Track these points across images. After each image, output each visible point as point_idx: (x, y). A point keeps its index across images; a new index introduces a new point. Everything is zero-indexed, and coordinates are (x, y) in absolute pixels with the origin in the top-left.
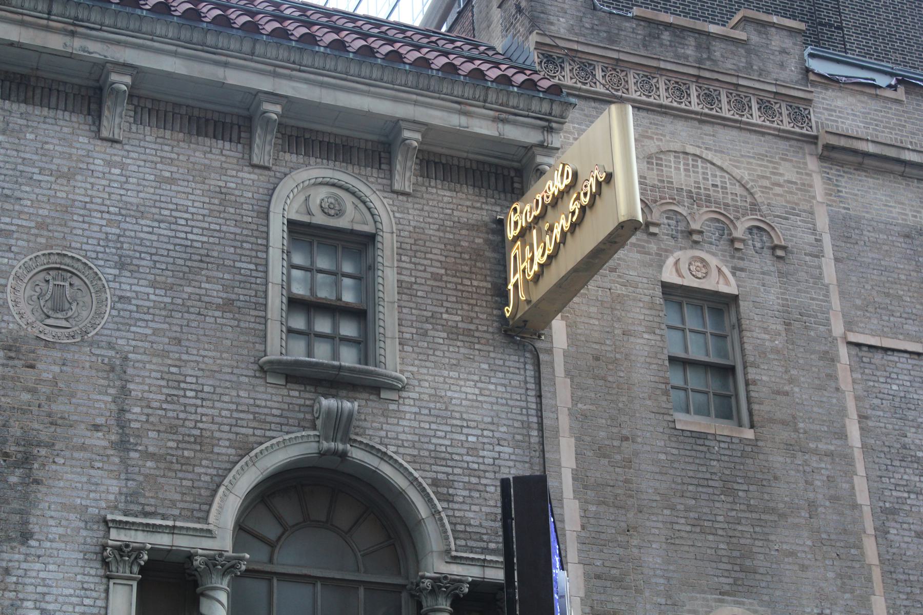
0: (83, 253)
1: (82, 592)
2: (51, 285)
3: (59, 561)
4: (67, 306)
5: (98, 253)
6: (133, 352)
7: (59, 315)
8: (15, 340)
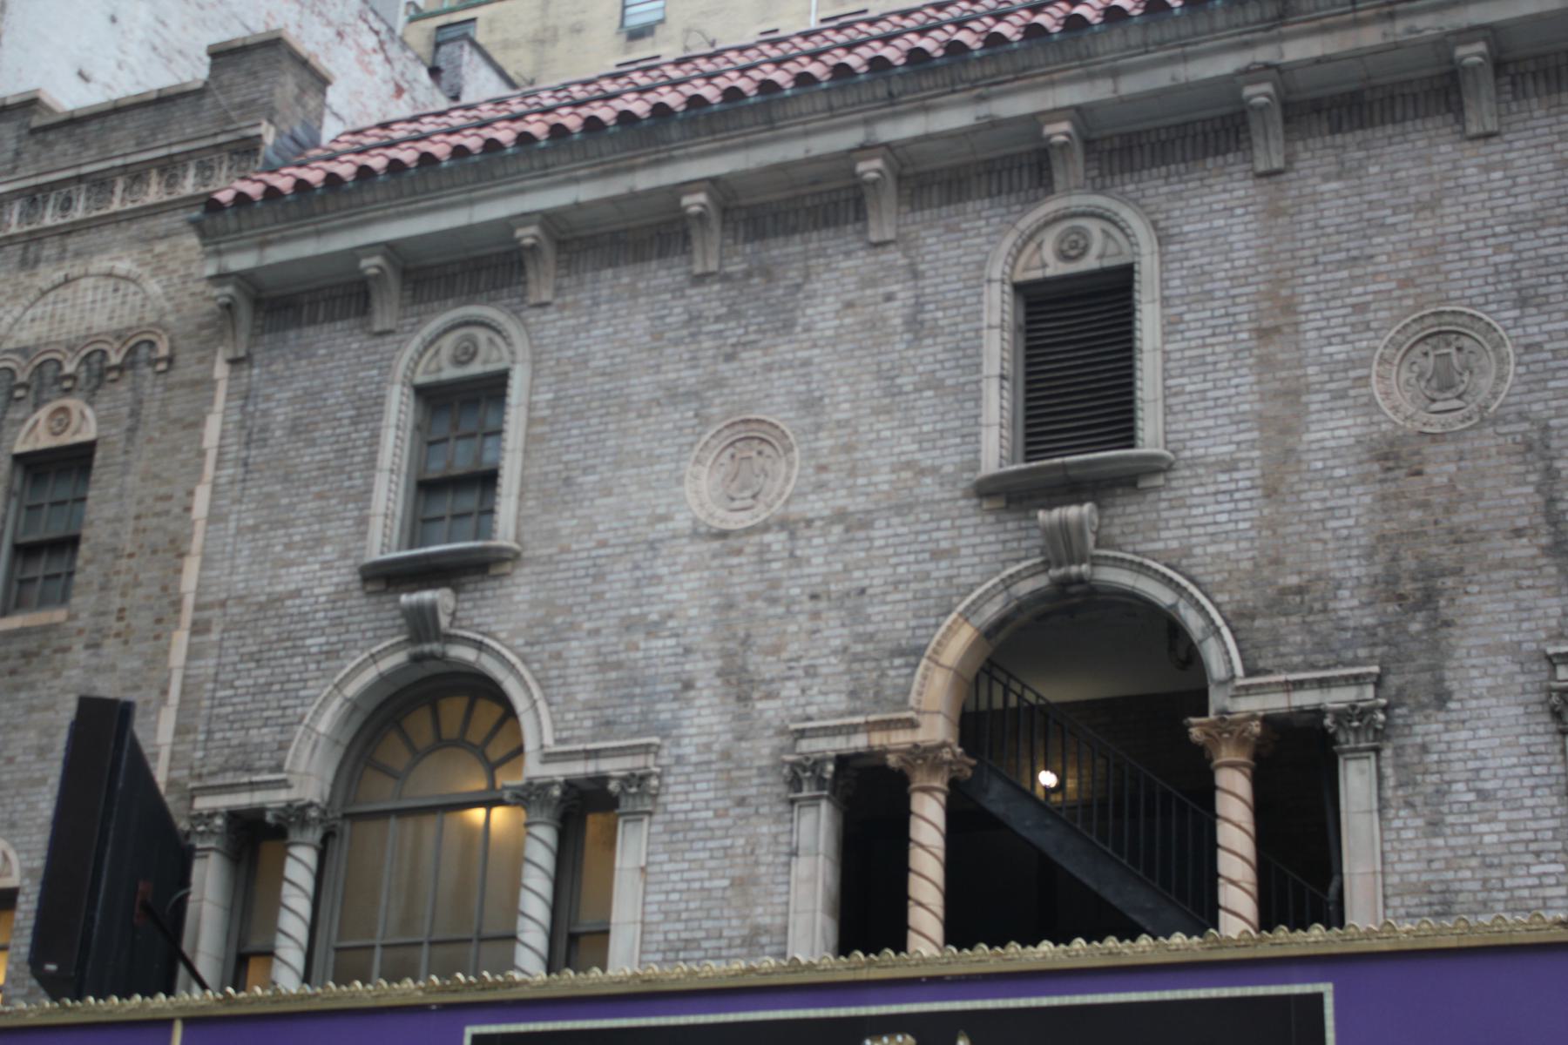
0: (1466, 301)
1: (1530, 759)
2: (1431, 358)
3: (1491, 723)
4: (1457, 378)
5: (1486, 295)
6: (1557, 416)
7: (1449, 395)
8: (1391, 444)
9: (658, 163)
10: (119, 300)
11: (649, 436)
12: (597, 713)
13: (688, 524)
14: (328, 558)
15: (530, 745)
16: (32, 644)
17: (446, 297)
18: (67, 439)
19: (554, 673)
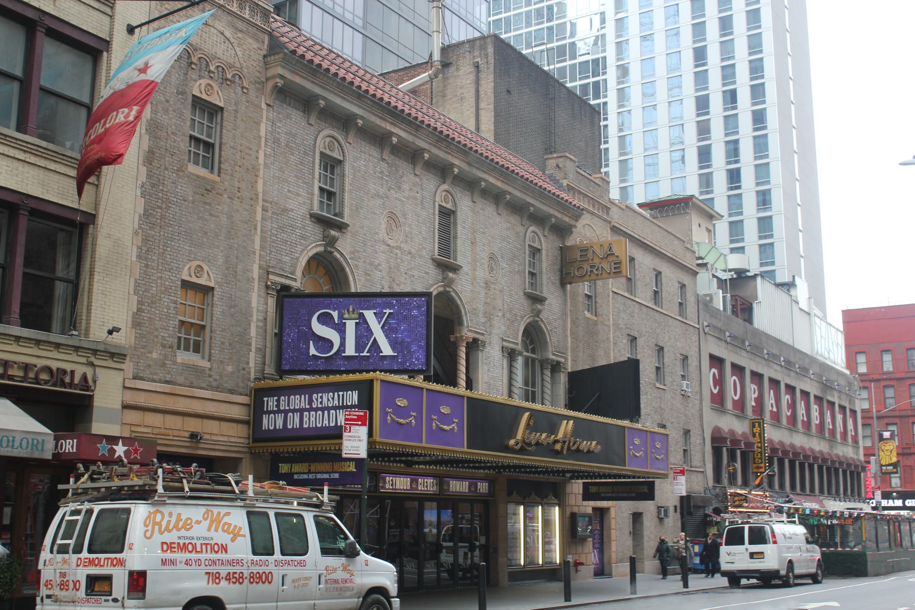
9: (392, 124)
16: (209, 187)
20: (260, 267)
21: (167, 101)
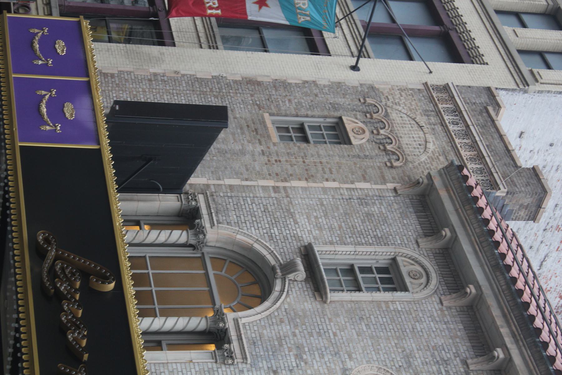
9: (514, 336)
10: (415, 146)
11: (387, 348)
12: (258, 338)
13: (349, 367)
14: (313, 232)
15: (240, 314)
16: (260, 132)
17: (438, 265)
18: (351, 135)
19: (274, 321)
20: (208, 186)
21: (316, 95)
